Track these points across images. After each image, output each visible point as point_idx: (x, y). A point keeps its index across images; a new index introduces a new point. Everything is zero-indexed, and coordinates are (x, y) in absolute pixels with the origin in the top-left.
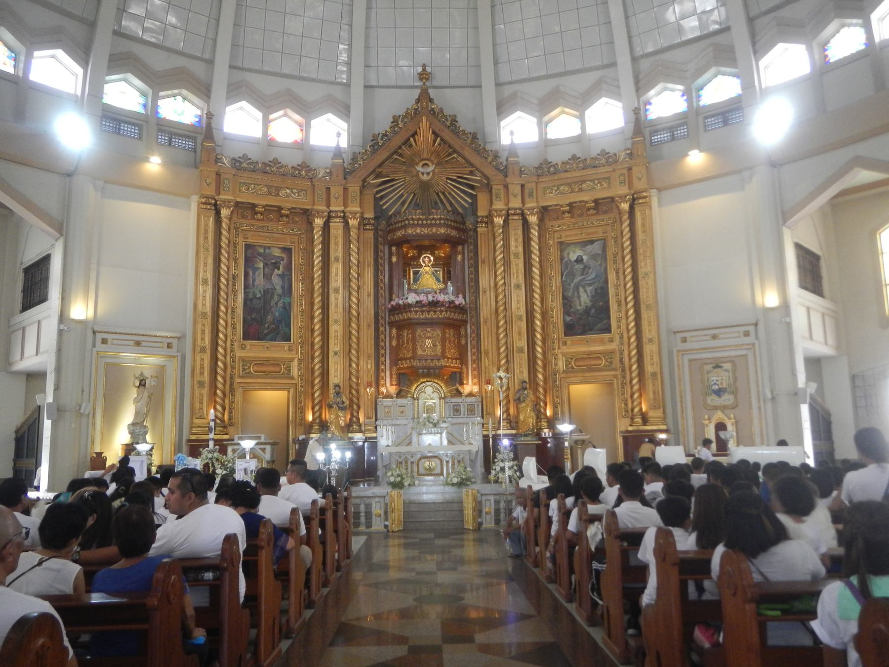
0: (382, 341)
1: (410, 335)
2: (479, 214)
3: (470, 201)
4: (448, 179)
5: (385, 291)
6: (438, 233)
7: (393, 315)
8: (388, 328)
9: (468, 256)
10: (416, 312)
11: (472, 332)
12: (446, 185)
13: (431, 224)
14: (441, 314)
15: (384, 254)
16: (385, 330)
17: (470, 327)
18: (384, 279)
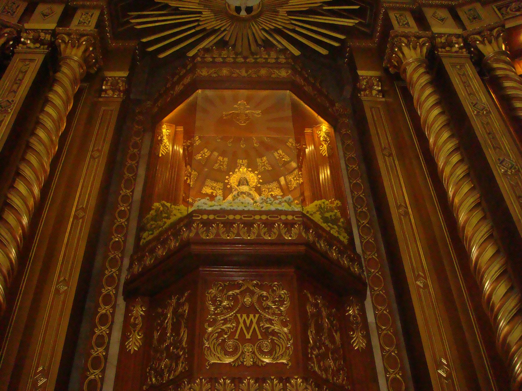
0: (99, 345)
1: (186, 308)
2: (360, 73)
3: (342, 37)
4: (290, 13)
5: (128, 220)
6: (273, 76)
7: (140, 260)
8: (121, 303)
9: (345, 157)
10: (207, 224)
11: (380, 318)
12: (287, 20)
13: (256, 63)
14: (289, 232)
15: (140, 151)
16: (113, 314)
17: (375, 308)
18: (132, 196)
